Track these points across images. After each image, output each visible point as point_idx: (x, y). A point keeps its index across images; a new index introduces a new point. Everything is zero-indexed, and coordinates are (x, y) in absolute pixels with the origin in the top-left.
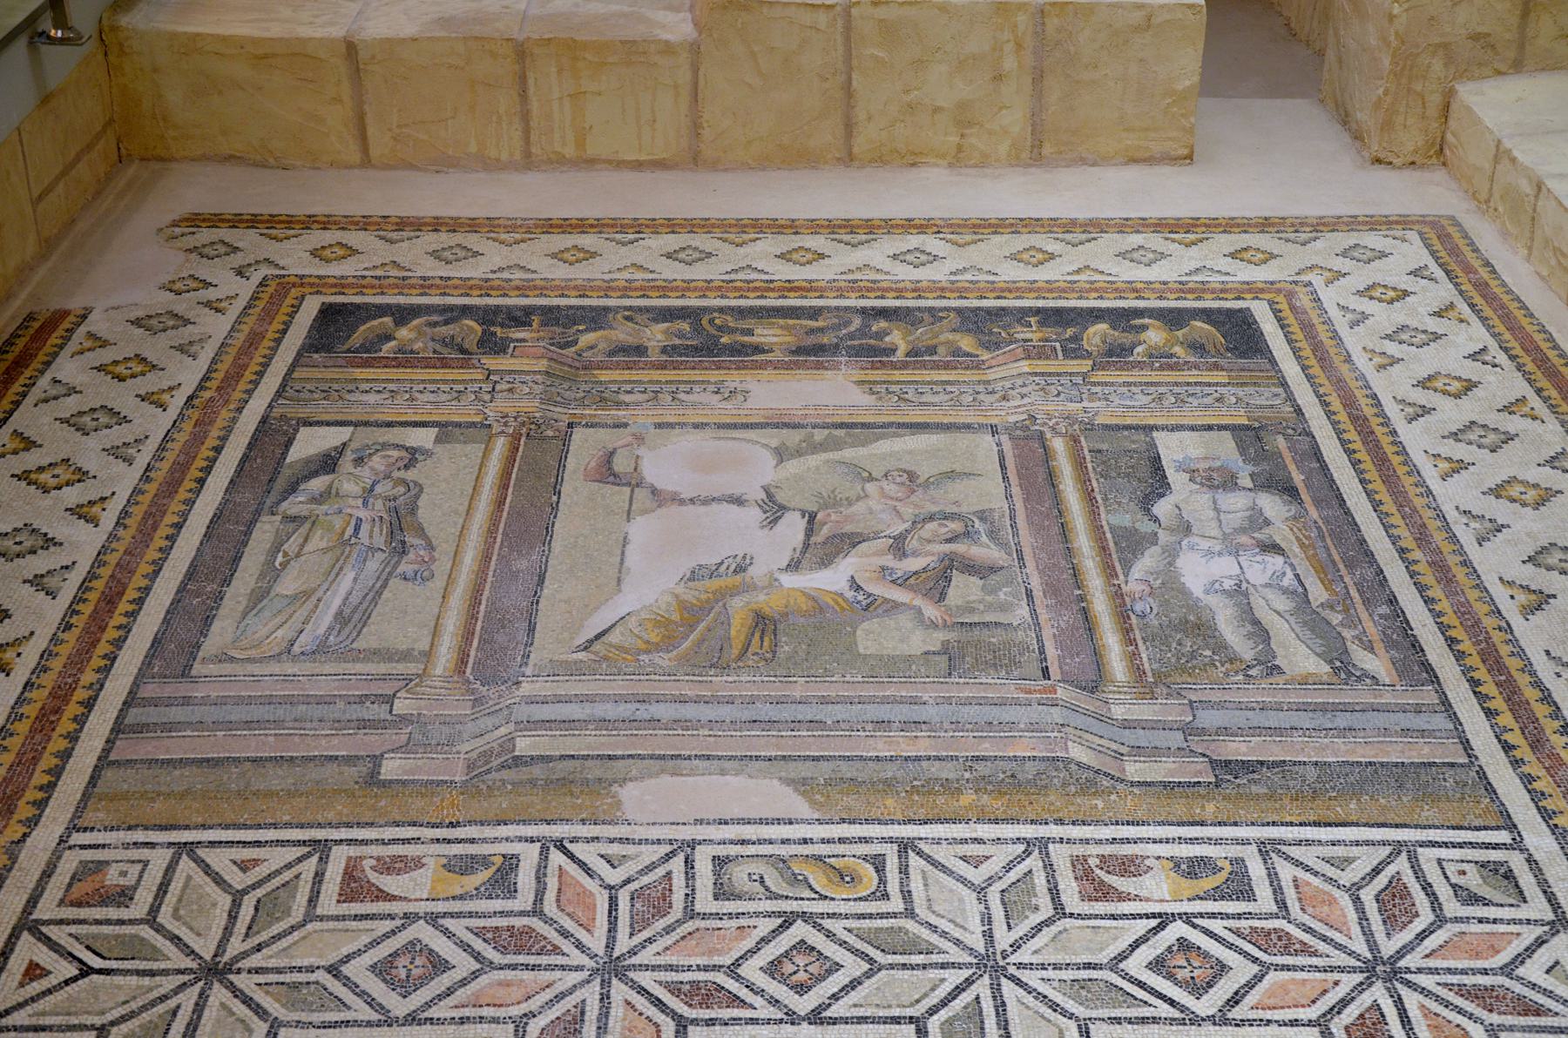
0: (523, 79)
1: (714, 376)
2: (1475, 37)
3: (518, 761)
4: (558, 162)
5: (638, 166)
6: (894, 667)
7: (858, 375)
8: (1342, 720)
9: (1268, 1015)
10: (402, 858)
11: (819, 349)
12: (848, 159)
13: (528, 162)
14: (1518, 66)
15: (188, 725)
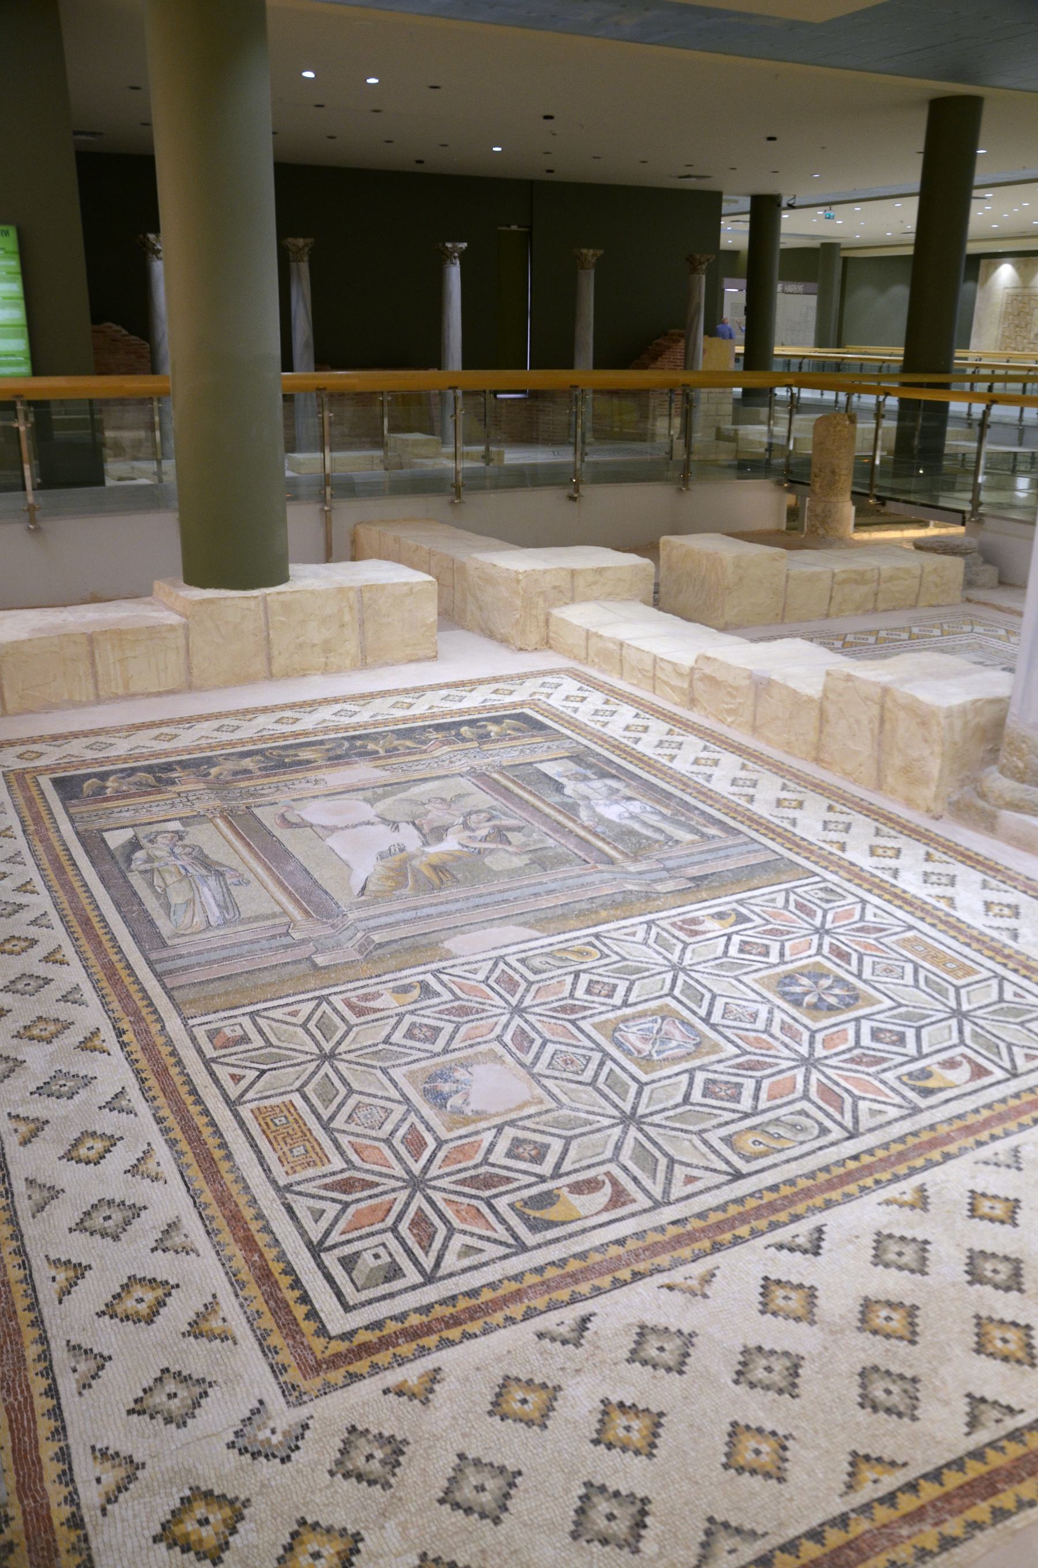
0: (92, 654)
1: (300, 775)
2: (555, 588)
3: (381, 945)
4: (116, 698)
5: (159, 694)
6: (514, 873)
8: (722, 853)
11: (339, 757)
12: (271, 676)
13: (98, 700)
14: (573, 600)
15: (199, 964)
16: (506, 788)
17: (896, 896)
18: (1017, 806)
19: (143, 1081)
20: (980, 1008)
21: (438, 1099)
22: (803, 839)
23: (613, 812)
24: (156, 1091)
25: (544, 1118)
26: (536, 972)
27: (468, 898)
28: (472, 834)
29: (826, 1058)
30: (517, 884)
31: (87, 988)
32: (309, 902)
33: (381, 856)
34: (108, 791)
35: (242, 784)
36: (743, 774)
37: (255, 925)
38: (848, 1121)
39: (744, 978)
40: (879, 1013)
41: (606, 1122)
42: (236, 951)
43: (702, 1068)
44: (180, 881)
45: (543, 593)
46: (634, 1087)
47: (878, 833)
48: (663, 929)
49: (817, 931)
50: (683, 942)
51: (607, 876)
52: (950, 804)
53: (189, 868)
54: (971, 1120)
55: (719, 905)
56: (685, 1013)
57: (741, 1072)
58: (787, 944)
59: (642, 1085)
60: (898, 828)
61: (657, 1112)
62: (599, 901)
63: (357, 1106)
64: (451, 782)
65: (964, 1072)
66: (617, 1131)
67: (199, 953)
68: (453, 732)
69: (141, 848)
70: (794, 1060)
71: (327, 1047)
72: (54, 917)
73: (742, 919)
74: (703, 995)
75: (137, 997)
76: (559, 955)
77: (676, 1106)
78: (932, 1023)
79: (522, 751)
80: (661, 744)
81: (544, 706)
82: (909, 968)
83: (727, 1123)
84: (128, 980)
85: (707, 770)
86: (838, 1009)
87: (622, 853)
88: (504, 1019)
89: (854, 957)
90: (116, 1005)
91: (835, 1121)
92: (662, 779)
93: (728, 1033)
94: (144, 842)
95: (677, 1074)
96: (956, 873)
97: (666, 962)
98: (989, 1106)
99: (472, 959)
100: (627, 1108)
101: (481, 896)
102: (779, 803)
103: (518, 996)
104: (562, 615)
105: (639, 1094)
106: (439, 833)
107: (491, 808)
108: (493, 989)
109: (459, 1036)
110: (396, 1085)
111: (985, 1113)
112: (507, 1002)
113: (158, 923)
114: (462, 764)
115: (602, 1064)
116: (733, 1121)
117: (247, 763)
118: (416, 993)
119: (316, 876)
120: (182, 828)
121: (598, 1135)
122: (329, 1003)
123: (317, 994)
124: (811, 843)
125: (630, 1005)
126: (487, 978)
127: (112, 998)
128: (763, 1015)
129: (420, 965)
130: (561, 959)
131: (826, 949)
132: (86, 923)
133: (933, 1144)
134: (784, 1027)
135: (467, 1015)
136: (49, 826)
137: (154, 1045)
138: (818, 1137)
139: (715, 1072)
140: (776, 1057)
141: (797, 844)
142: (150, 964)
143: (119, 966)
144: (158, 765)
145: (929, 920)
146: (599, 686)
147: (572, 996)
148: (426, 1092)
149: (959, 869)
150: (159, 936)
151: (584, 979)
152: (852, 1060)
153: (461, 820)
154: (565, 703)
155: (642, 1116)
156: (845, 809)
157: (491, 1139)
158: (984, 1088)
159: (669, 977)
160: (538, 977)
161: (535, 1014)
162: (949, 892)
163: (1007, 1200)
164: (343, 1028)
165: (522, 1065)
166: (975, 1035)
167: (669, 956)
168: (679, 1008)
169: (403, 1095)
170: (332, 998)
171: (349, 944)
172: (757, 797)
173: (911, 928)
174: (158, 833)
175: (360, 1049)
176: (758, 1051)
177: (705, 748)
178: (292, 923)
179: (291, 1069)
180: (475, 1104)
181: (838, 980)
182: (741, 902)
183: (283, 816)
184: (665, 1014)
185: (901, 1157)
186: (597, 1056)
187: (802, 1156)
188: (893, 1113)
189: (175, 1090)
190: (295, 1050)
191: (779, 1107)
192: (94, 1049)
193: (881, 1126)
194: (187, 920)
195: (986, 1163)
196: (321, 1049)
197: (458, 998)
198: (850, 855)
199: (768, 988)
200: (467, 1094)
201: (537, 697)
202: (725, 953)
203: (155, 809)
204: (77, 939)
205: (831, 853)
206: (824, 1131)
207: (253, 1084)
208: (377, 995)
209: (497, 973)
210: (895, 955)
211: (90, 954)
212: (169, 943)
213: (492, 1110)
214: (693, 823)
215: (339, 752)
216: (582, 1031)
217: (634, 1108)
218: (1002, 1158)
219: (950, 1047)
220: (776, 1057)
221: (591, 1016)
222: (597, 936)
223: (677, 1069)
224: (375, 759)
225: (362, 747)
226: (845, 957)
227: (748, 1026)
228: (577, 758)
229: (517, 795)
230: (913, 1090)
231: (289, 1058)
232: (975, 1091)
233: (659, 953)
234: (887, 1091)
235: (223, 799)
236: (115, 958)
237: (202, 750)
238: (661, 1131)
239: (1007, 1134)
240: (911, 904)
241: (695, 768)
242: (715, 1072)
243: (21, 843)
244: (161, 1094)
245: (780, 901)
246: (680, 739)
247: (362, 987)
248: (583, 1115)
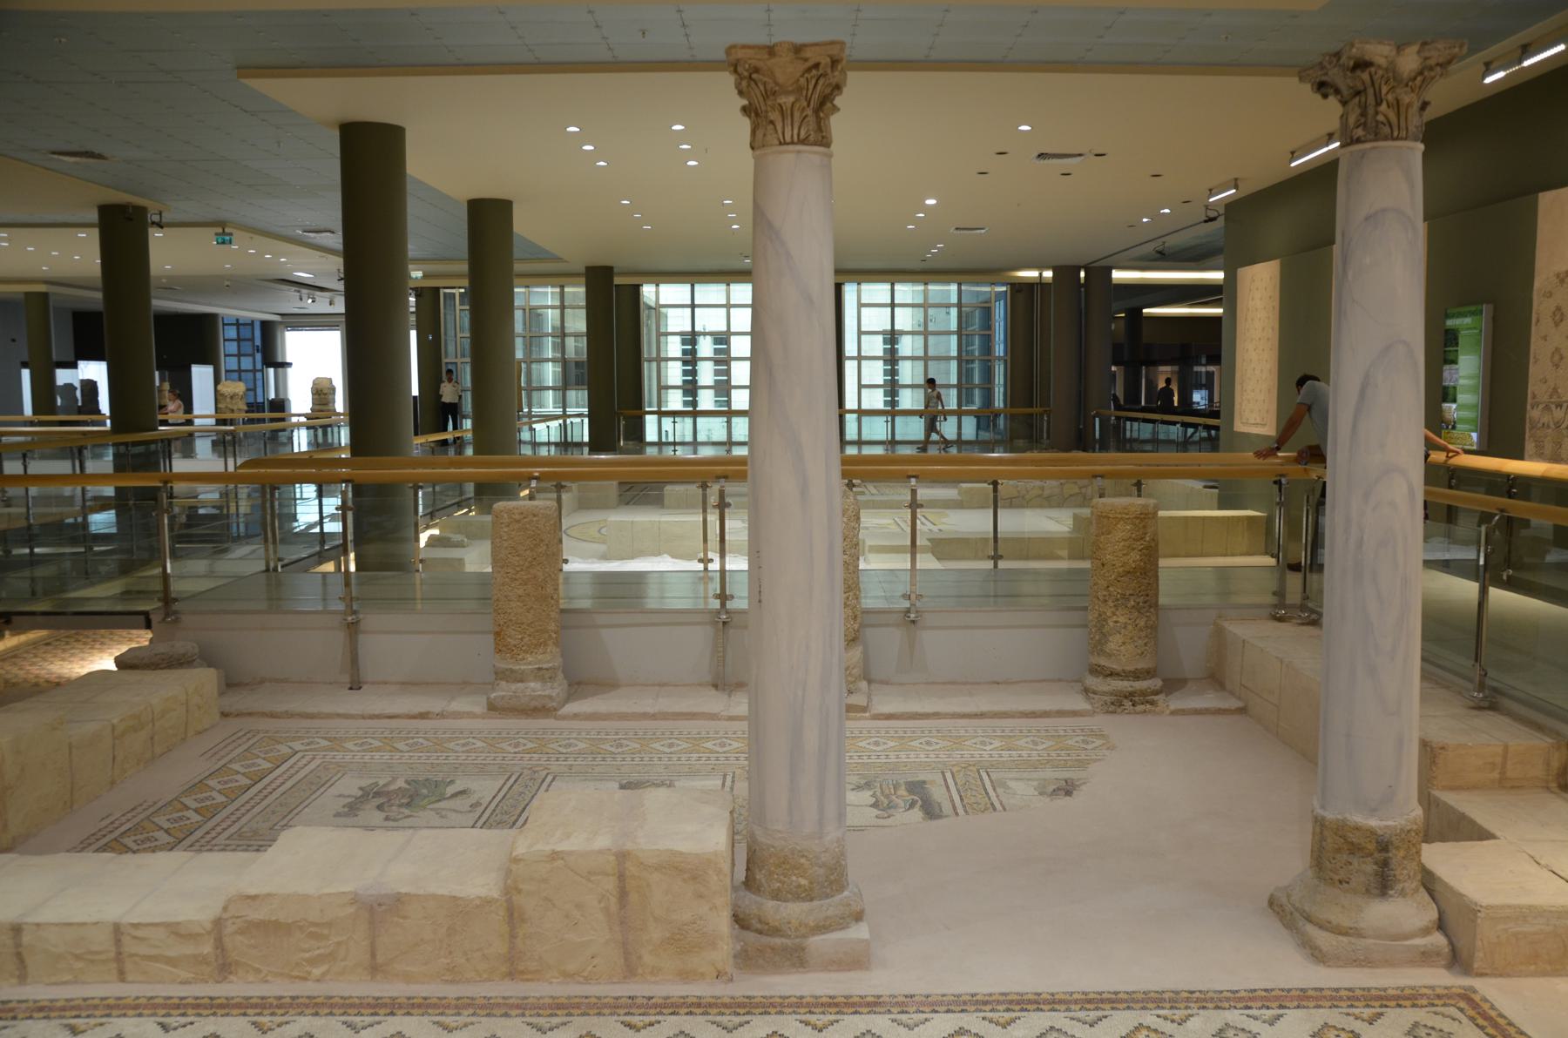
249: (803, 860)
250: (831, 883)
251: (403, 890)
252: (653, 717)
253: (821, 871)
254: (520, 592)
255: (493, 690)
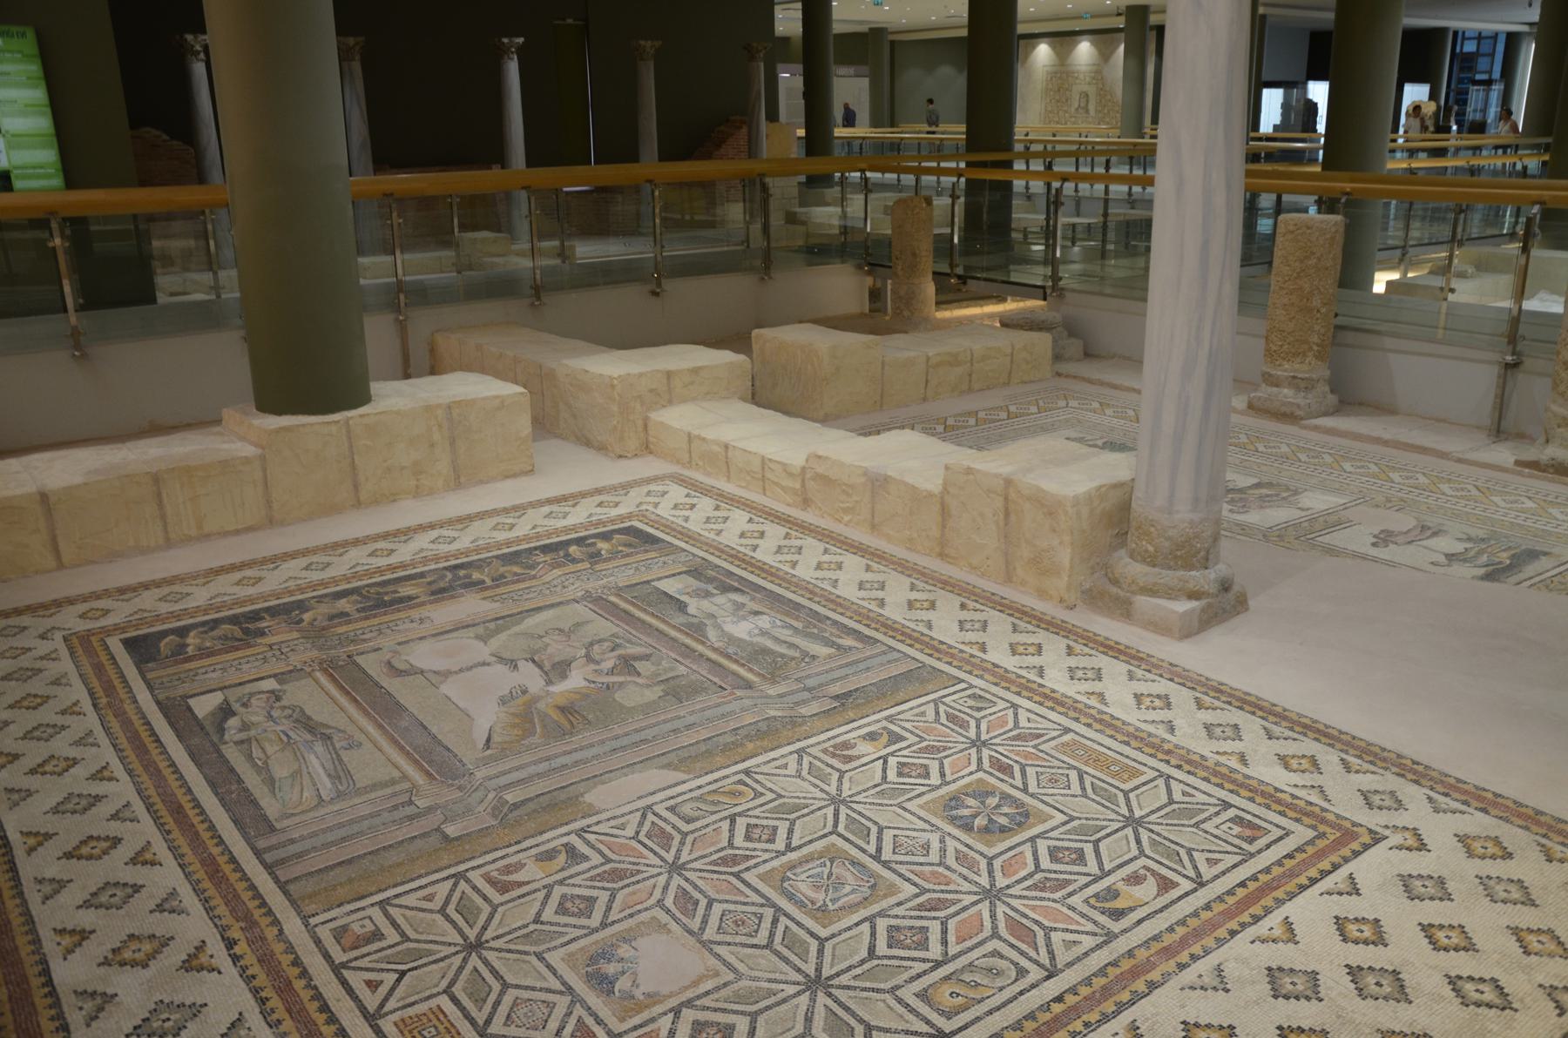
0: (159, 495)
1: (402, 615)
2: (651, 391)
3: (516, 806)
4: (188, 540)
5: (237, 532)
6: (647, 709)
7: (479, 596)
8: (862, 666)
9: (960, 774)
10: (510, 865)
11: (442, 590)
12: (358, 504)
13: (169, 544)
14: (670, 402)
15: (315, 849)
16: (625, 611)
17: (1046, 696)
18: (1151, 590)
19: (263, 1002)
20: (1153, 812)
21: (604, 984)
22: (941, 643)
23: (742, 629)
24: (281, 1013)
25: (724, 993)
26: (689, 821)
27: (603, 742)
28: (597, 667)
29: (1008, 887)
30: (653, 721)
31: (185, 891)
32: (430, 762)
33: (503, 701)
34: (190, 649)
35: (341, 630)
36: (869, 576)
37: (373, 795)
38: (1044, 958)
39: (908, 805)
40: (1052, 830)
41: (791, 990)
42: (356, 828)
43: (882, 914)
44: (283, 750)
45: (640, 397)
46: (814, 945)
47: (1015, 629)
48: (815, 758)
49: (973, 744)
50: (838, 770)
51: (747, 702)
52: (1083, 592)
53: (291, 734)
54: (1168, 940)
55: (869, 724)
56: (854, 852)
57: (923, 914)
58: (946, 762)
59: (822, 942)
60: (1034, 622)
61: (843, 972)
62: (742, 732)
63: (515, 1004)
64: (567, 609)
65: (1150, 886)
66: (804, 999)
67: (314, 835)
68: (561, 553)
69: (234, 714)
70: (975, 893)
71: (472, 934)
72: (139, 808)
73: (895, 738)
74: (869, 829)
75: (246, 896)
76: (710, 798)
77: (863, 962)
78: (1108, 835)
79: (637, 569)
80: (779, 550)
81: (653, 517)
82: (1073, 775)
83: (919, 976)
84: (233, 877)
85: (832, 575)
86: (1010, 829)
87: (759, 675)
88: (662, 880)
89: (1017, 768)
90: (222, 910)
91: (1030, 959)
92: (786, 588)
93: (902, 869)
94: (236, 707)
95: (857, 924)
96: (1101, 665)
97: (825, 796)
98: (1182, 922)
99: (618, 812)
100: (810, 969)
101: (616, 738)
102: (911, 605)
103: (673, 850)
104: (660, 419)
105: (821, 952)
106: (561, 669)
107: (613, 635)
108: (645, 846)
109: (616, 905)
110: (554, 972)
111: (1180, 931)
112: (662, 859)
113: (263, 803)
114: (576, 589)
115: (775, 921)
116: (925, 973)
117: (343, 605)
118: (562, 858)
119: (434, 730)
120: (278, 687)
121: (784, 1007)
122: (468, 881)
123: (452, 871)
124: (950, 647)
125: (794, 849)
126: (637, 833)
127: (217, 901)
128: (935, 845)
129: (562, 825)
130: (714, 803)
131: (986, 764)
132: (178, 811)
133: (1135, 973)
134: (959, 857)
135: (622, 879)
136: (123, 696)
137: (272, 954)
138: (1016, 980)
139: (897, 916)
140: (957, 892)
141: (936, 648)
142: (258, 853)
143: (221, 860)
144: (243, 615)
145: (1084, 720)
146: (706, 491)
147: (731, 845)
148: (589, 978)
149: (1102, 661)
150: (265, 818)
151: (741, 823)
152: (1035, 887)
153: (583, 651)
154: (674, 512)
155: (828, 978)
156: (978, 606)
157: (669, 1026)
158: (1173, 902)
159: (830, 811)
160: (691, 827)
161: (695, 870)
162: (1097, 687)
163: (1221, 1027)
164: (487, 909)
165: (690, 932)
166: (1153, 843)
167: (826, 788)
168: (847, 846)
169: (564, 983)
170: (470, 875)
171: (481, 808)
172: (887, 600)
173: (1067, 730)
174: (252, 695)
175: (509, 933)
176: (937, 887)
177: (826, 551)
178: (414, 789)
179: (434, 966)
180: (646, 986)
181: (1005, 797)
182: (890, 719)
183: (389, 663)
184: (833, 855)
185: (1106, 992)
186: (769, 913)
187: (1004, 1005)
188: (1088, 942)
189: (304, 1009)
190: (436, 942)
191: (970, 949)
192: (201, 969)
193: (1079, 959)
194: (295, 797)
195: (1192, 988)
196: (465, 938)
197: (609, 861)
198: (992, 656)
199: (935, 814)
200: (635, 974)
201: (644, 507)
202: (884, 778)
203: (245, 667)
204: (169, 832)
205: (972, 656)
206: (1022, 972)
207: (393, 989)
208: (520, 866)
209: (647, 826)
210: (1057, 763)
211: (186, 849)
212: (278, 826)
213: (665, 991)
214: (827, 635)
215: (442, 584)
216: (748, 885)
217: (819, 970)
218: (1207, 980)
219: (1132, 860)
220: (957, 892)
221: (756, 866)
222: (747, 772)
223: (855, 918)
224: (483, 590)
225: (466, 576)
226: (1006, 770)
227: (922, 860)
228: (695, 572)
229: (639, 619)
230: (1103, 913)
231: (430, 953)
232: (1166, 907)
233: (816, 786)
234: (1077, 918)
235: (320, 649)
236: (216, 851)
237: (291, 593)
238: (851, 993)
239: (1207, 952)
240: (1062, 704)
241: (820, 574)
242: (897, 916)
243: (92, 720)
244: (287, 1016)
245: (931, 715)
246: (798, 543)
247: (502, 858)
248: (766, 985)
249: (1152, 529)
250: (1176, 557)
251: (889, 473)
252: (1386, 443)
253: (1167, 544)
254: (1286, 301)
255: (1255, 390)
